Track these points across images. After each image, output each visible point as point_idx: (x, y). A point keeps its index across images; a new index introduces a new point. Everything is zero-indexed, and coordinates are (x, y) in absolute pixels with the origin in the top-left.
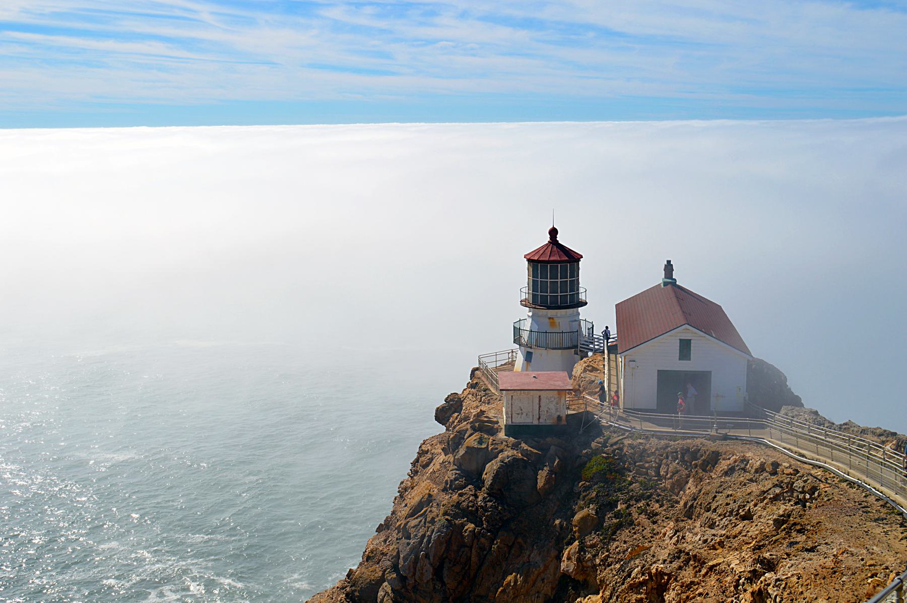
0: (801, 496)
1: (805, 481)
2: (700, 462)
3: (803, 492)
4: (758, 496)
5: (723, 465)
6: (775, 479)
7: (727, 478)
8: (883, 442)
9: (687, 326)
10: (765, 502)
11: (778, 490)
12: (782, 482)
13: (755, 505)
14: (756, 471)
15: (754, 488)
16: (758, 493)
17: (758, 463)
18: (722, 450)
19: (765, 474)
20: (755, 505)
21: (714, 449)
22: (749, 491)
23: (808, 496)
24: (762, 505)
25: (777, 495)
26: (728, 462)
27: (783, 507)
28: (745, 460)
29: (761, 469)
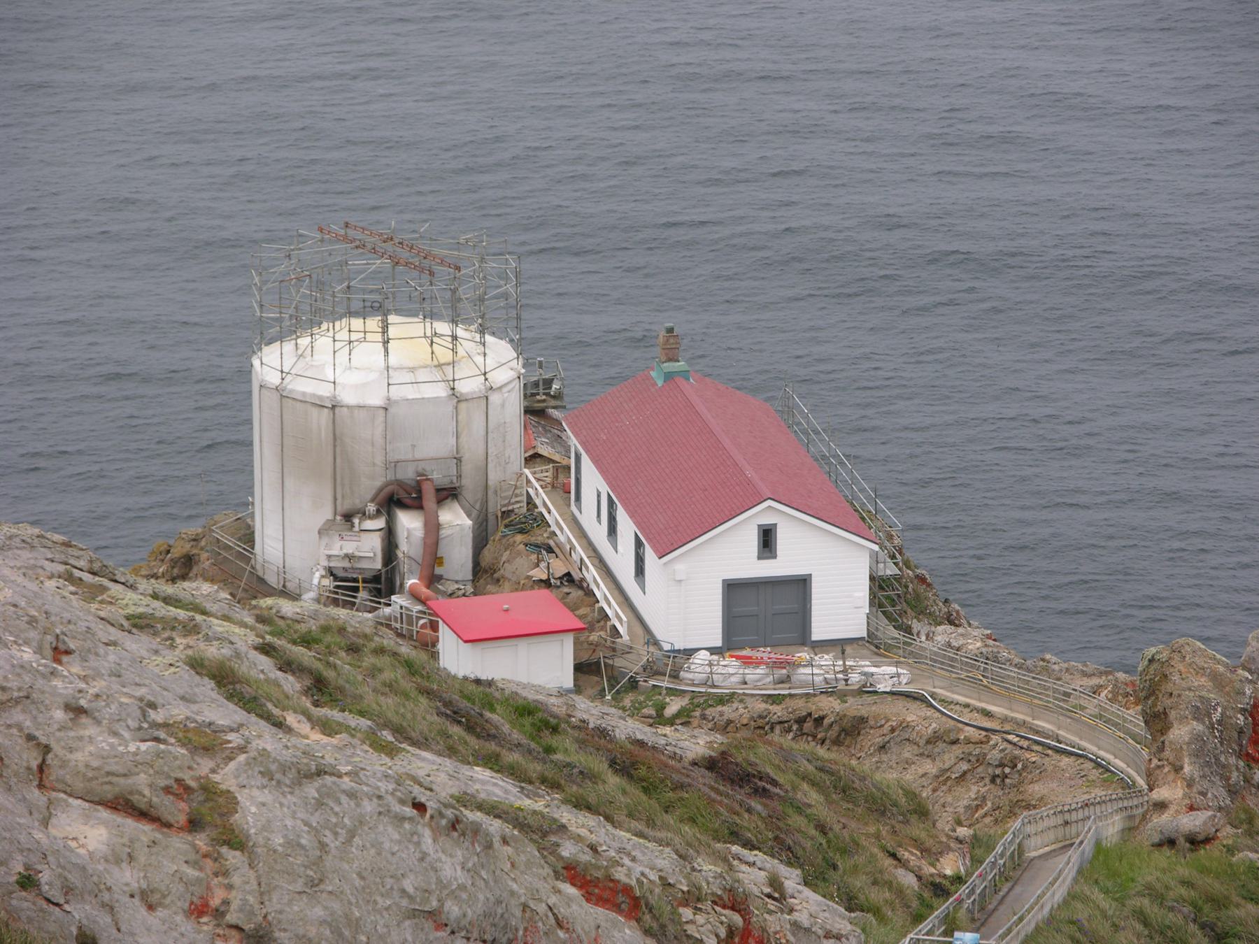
0: (998, 771)
1: (1003, 750)
2: (833, 733)
3: (1002, 765)
4: (937, 777)
5: (872, 738)
6: (957, 750)
7: (885, 757)
8: (1096, 691)
9: (770, 503)
10: (949, 783)
11: (965, 766)
12: (970, 754)
13: (934, 791)
14: (928, 742)
15: (930, 767)
16: (934, 771)
17: (930, 731)
18: (864, 712)
19: (941, 745)
20: (934, 791)
21: (852, 712)
22: (921, 771)
23: (1007, 770)
24: (944, 788)
25: (965, 773)
26: (881, 732)
27: (974, 788)
28: (904, 726)
29: (934, 739)
